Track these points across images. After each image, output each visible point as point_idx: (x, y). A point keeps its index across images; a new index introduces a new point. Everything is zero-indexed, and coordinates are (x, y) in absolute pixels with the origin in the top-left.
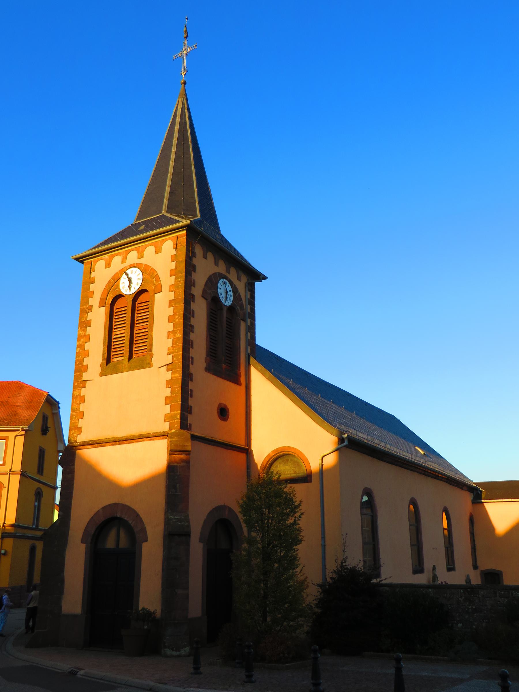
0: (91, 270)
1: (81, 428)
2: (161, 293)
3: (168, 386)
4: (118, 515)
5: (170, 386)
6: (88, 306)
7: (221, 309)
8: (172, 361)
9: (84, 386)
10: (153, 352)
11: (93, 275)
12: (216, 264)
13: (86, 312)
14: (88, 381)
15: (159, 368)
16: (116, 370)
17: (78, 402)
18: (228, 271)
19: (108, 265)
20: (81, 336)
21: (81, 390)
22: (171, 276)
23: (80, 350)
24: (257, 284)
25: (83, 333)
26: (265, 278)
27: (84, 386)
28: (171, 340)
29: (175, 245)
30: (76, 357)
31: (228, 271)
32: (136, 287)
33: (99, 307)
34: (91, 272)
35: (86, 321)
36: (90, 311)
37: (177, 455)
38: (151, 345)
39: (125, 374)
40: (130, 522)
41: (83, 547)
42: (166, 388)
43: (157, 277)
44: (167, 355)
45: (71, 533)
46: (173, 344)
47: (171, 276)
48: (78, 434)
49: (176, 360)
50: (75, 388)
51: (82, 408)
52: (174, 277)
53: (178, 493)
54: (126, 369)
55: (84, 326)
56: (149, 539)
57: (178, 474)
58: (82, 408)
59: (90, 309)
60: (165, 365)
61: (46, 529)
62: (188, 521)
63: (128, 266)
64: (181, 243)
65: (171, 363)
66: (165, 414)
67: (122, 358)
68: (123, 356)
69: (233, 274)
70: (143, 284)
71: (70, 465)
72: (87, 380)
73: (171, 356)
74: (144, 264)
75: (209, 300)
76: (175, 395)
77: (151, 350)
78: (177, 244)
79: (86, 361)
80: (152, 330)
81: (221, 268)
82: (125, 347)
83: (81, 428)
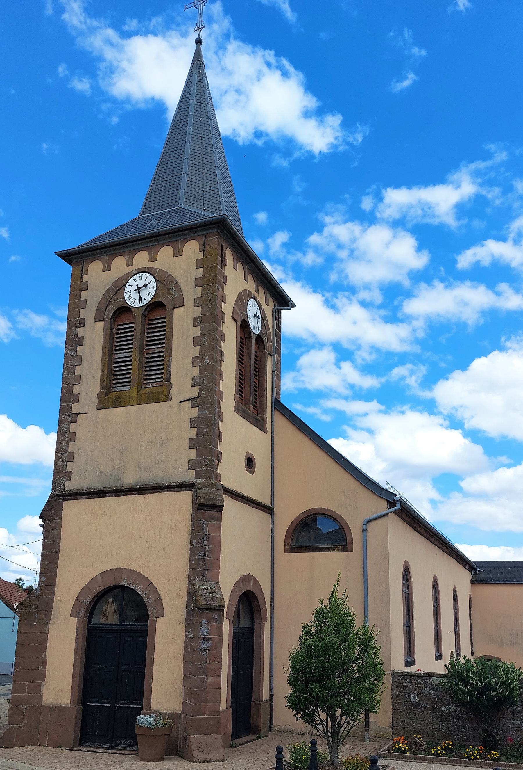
0: (83, 273)
1: (70, 473)
2: (183, 307)
3: (194, 425)
4: (124, 583)
5: (196, 426)
6: (78, 319)
7: (250, 337)
8: (198, 394)
9: (75, 421)
10: (172, 381)
11: (85, 278)
12: (246, 280)
13: (76, 327)
14: (80, 415)
15: (180, 402)
16: (118, 403)
17: (66, 440)
18: (257, 291)
19: (107, 268)
20: (70, 357)
21: (70, 425)
22: (196, 286)
23: (68, 374)
24: (285, 313)
25: (72, 353)
26: (293, 306)
27: (75, 421)
28: (197, 369)
29: (202, 246)
30: (63, 383)
31: (257, 291)
32: (148, 296)
33: (95, 321)
34: (83, 274)
35: (76, 338)
36: (82, 325)
37: (206, 510)
38: (170, 373)
39: (133, 408)
40: (140, 593)
41: (74, 622)
42: (191, 428)
43: (177, 285)
44: (192, 387)
45: (56, 603)
46: (200, 373)
47: (196, 286)
48: (67, 480)
49: (204, 393)
50: (61, 423)
51: (71, 447)
52: (201, 288)
53: (207, 558)
54: (134, 401)
55: (74, 344)
56: (166, 613)
57: (207, 534)
58: (71, 447)
59: (83, 322)
60: (189, 400)
61: (137, 717)
62: (220, 593)
63: (136, 271)
64: (211, 244)
65: (198, 397)
66: (189, 460)
67: (129, 388)
68: (130, 385)
69: (261, 295)
70: (157, 295)
71: (56, 518)
72: (79, 414)
73: (197, 389)
74: (158, 270)
75: (239, 323)
76: (203, 436)
77: (169, 380)
78: (204, 246)
79: (76, 389)
80: (170, 355)
81: (250, 285)
82: (133, 374)
83: (70, 473)
